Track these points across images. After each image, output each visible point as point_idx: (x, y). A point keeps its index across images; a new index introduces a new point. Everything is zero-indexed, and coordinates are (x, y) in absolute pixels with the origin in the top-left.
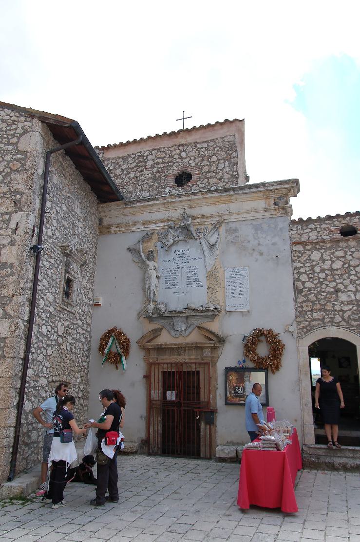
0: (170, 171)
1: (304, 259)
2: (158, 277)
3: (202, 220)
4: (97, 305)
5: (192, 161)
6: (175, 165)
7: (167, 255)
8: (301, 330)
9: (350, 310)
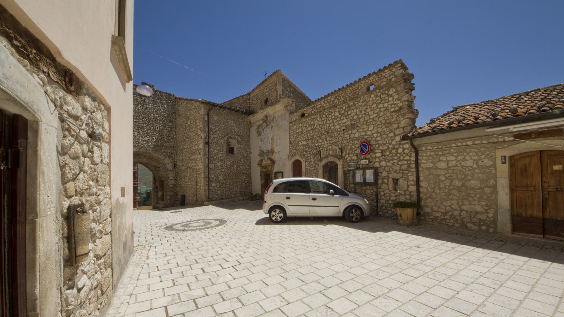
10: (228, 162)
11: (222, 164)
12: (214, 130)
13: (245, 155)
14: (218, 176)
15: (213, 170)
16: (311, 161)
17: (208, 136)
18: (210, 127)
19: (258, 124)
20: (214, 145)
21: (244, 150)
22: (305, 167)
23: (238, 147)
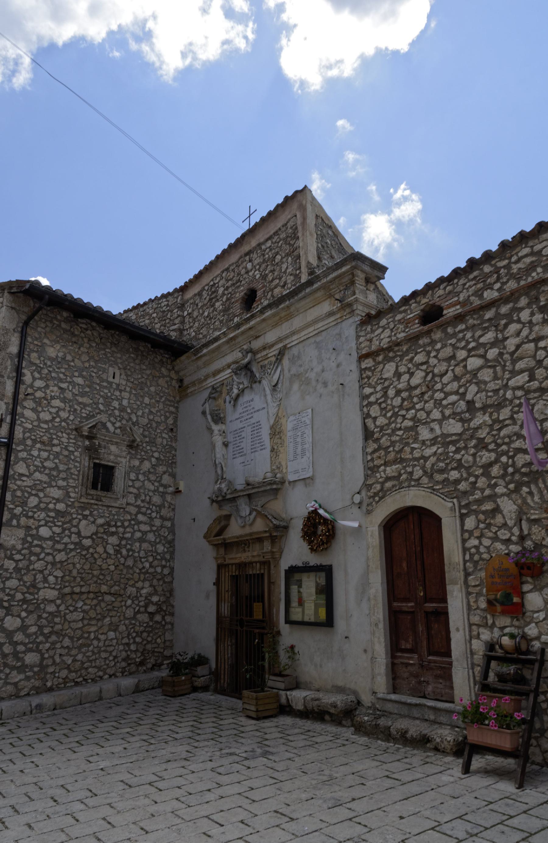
1: (375, 380)
2: (226, 445)
3: (264, 353)
4: (178, 491)
8: (371, 500)
9: (435, 453)
10: (84, 522)
11: (57, 530)
12: (39, 394)
13: (157, 499)
14: (34, 586)
15: (18, 557)
16: (497, 510)
17: (13, 413)
18: (27, 378)
19: (211, 382)
20: (35, 453)
21: (153, 478)
22: (464, 541)
23: (132, 468)
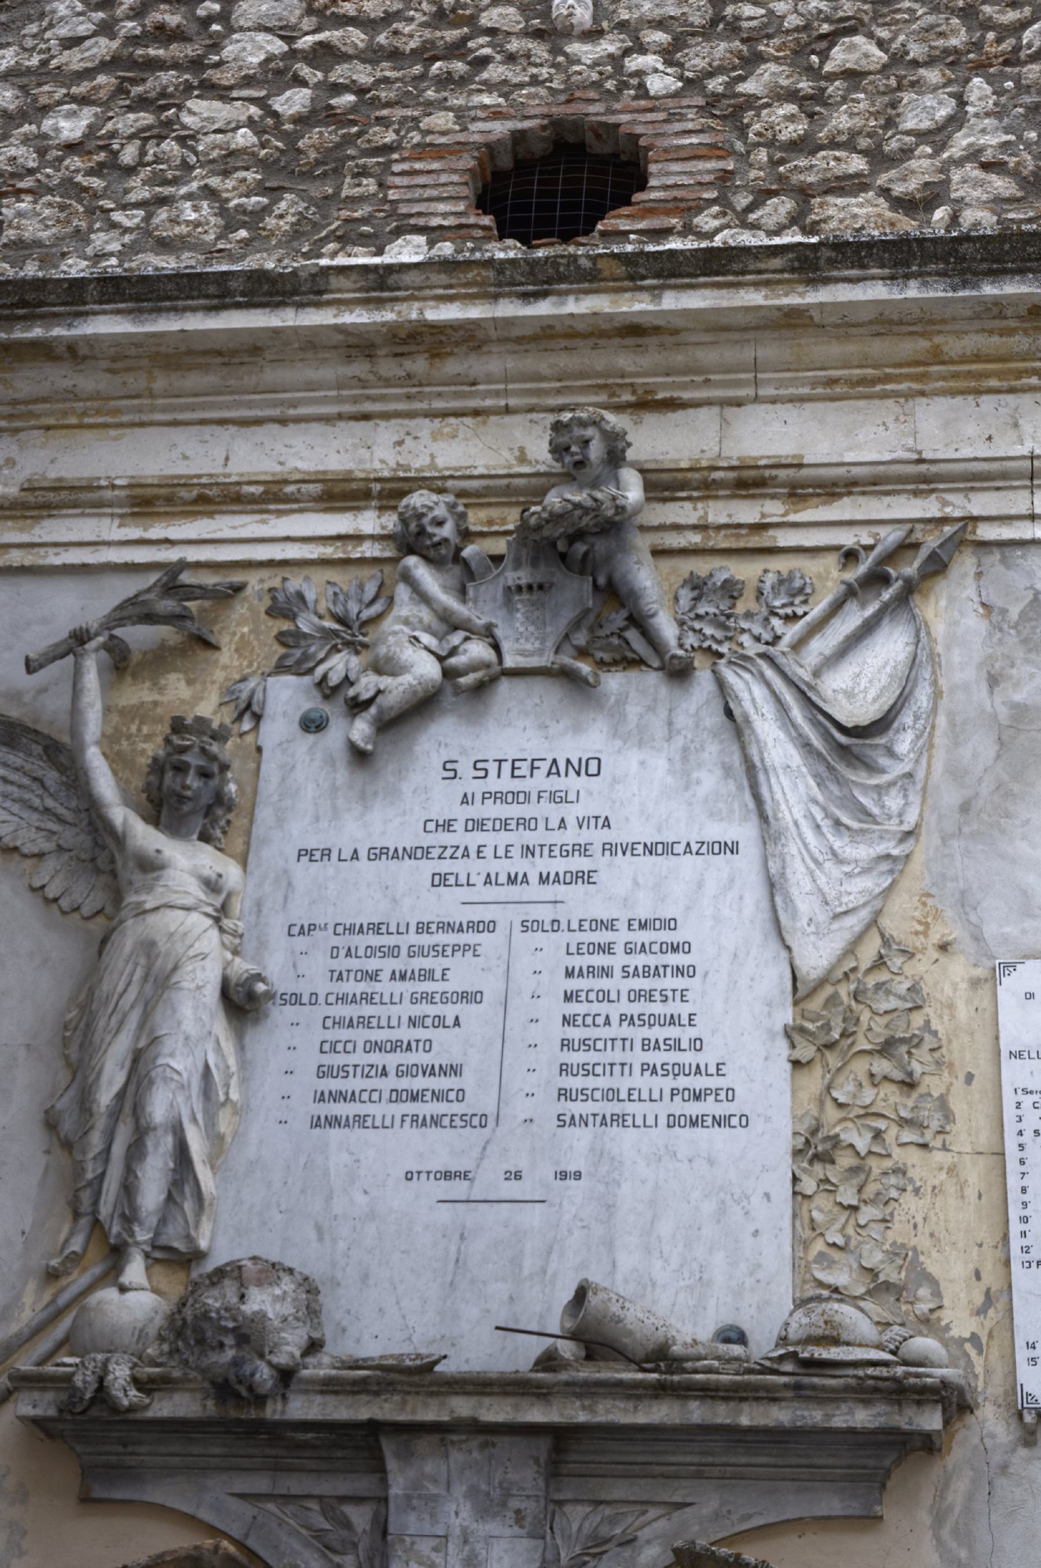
0: (443, 120)
3: (747, 512)
5: (650, 60)
6: (495, 72)
7: (364, 799)
